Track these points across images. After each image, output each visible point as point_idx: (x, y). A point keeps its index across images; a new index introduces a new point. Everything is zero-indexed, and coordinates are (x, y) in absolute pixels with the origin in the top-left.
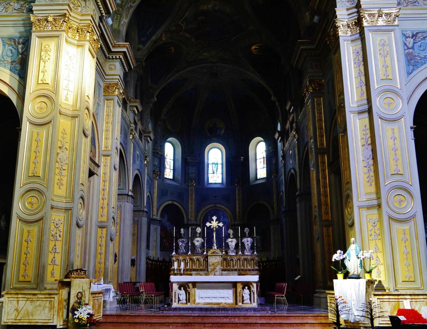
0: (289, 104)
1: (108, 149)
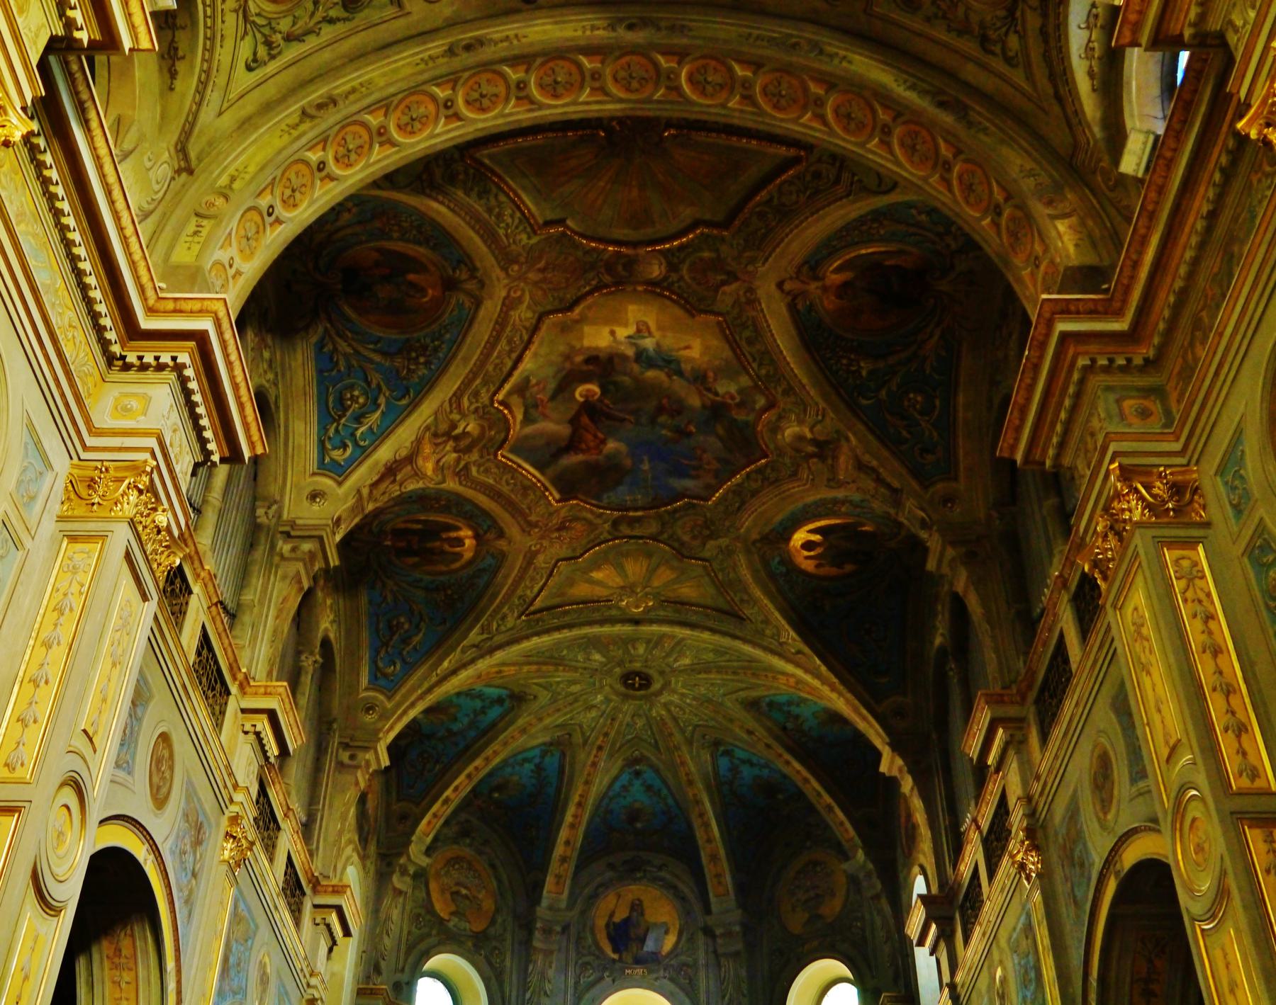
0: (983, 717)
1: (19, 773)
